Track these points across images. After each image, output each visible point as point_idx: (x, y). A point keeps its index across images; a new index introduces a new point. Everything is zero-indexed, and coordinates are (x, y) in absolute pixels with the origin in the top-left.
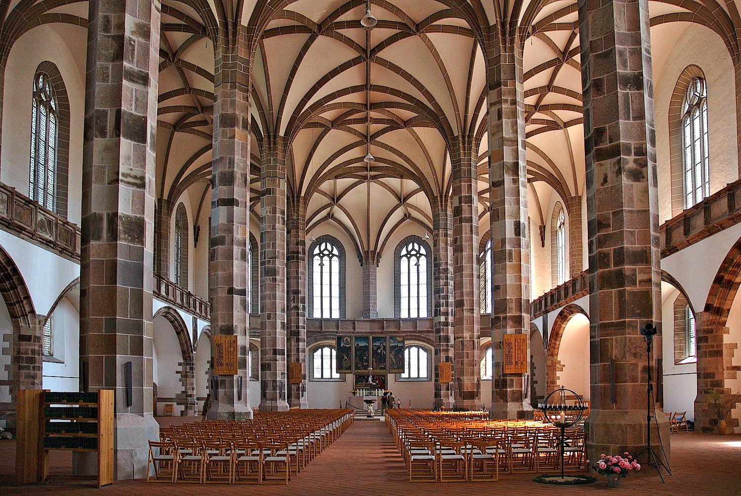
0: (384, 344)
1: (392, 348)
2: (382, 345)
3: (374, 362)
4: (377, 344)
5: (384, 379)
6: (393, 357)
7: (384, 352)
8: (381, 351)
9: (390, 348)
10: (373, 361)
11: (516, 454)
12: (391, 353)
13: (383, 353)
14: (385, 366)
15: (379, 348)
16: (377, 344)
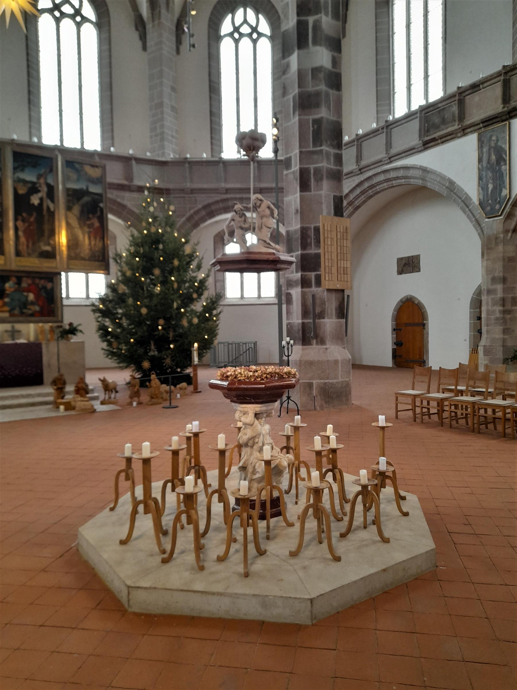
0: (50, 181)
1: (74, 196)
2: (42, 181)
3: (21, 233)
4: (29, 176)
5: (52, 289)
6: (74, 223)
7: (51, 206)
8: (41, 199)
9: (68, 195)
10: (16, 229)
11: (112, 399)
12: (69, 208)
13: (48, 208)
14: (54, 248)
15: (34, 189)
16: (29, 176)
